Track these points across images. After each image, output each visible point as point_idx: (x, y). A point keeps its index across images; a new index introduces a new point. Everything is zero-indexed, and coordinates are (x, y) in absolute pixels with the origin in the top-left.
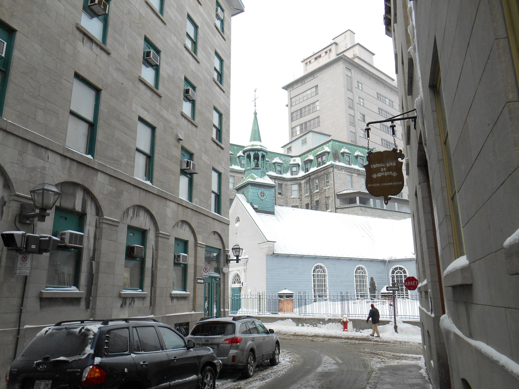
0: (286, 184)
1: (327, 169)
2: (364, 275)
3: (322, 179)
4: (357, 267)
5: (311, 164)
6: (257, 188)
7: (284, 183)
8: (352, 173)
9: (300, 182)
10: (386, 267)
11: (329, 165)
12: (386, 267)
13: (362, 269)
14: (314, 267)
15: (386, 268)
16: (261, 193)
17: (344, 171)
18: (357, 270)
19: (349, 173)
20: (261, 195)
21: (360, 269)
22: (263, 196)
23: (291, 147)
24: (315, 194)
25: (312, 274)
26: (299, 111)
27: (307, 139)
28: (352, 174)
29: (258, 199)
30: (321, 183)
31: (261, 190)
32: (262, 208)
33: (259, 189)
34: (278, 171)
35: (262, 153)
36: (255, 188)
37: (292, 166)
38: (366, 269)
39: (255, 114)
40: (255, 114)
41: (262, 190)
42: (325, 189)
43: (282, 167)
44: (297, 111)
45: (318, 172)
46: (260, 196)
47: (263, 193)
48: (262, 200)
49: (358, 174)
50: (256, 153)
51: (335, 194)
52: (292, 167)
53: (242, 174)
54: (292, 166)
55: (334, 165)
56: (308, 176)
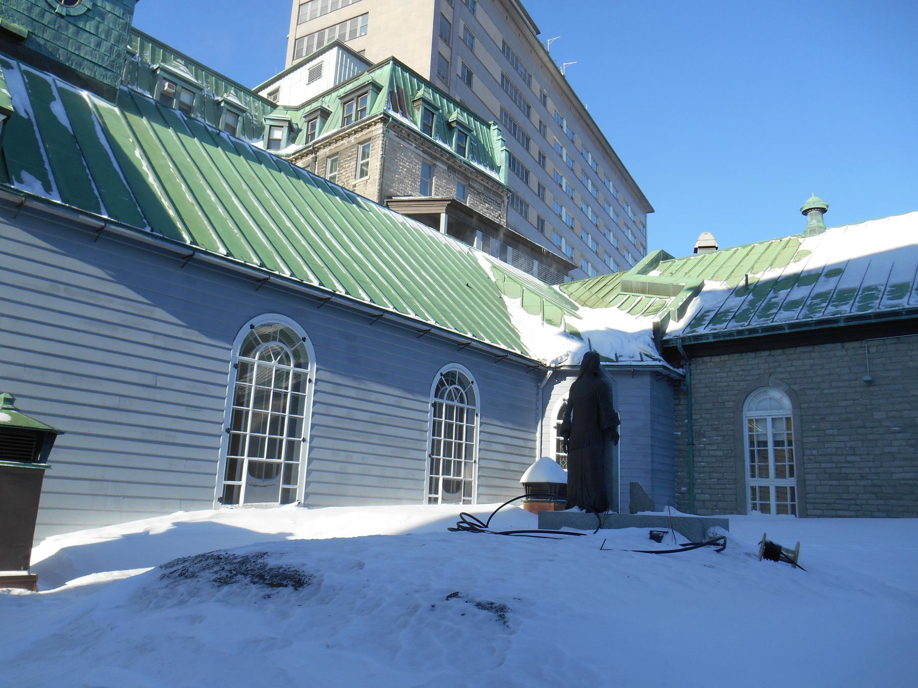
1: (369, 125)
2: (465, 406)
3: (349, 156)
4: (445, 369)
5: (324, 123)
8: (435, 158)
10: (540, 392)
11: (376, 116)
12: (540, 392)
13: (463, 382)
14: (248, 325)
15: (541, 394)
17: (414, 145)
18: (441, 383)
19: (426, 156)
21: (453, 383)
23: (277, 91)
26: (316, 35)
27: (324, 65)
28: (434, 162)
30: (345, 168)
38: (475, 388)
44: (311, 35)
45: (343, 138)
49: (450, 168)
52: (271, 126)
55: (389, 117)
56: (311, 152)
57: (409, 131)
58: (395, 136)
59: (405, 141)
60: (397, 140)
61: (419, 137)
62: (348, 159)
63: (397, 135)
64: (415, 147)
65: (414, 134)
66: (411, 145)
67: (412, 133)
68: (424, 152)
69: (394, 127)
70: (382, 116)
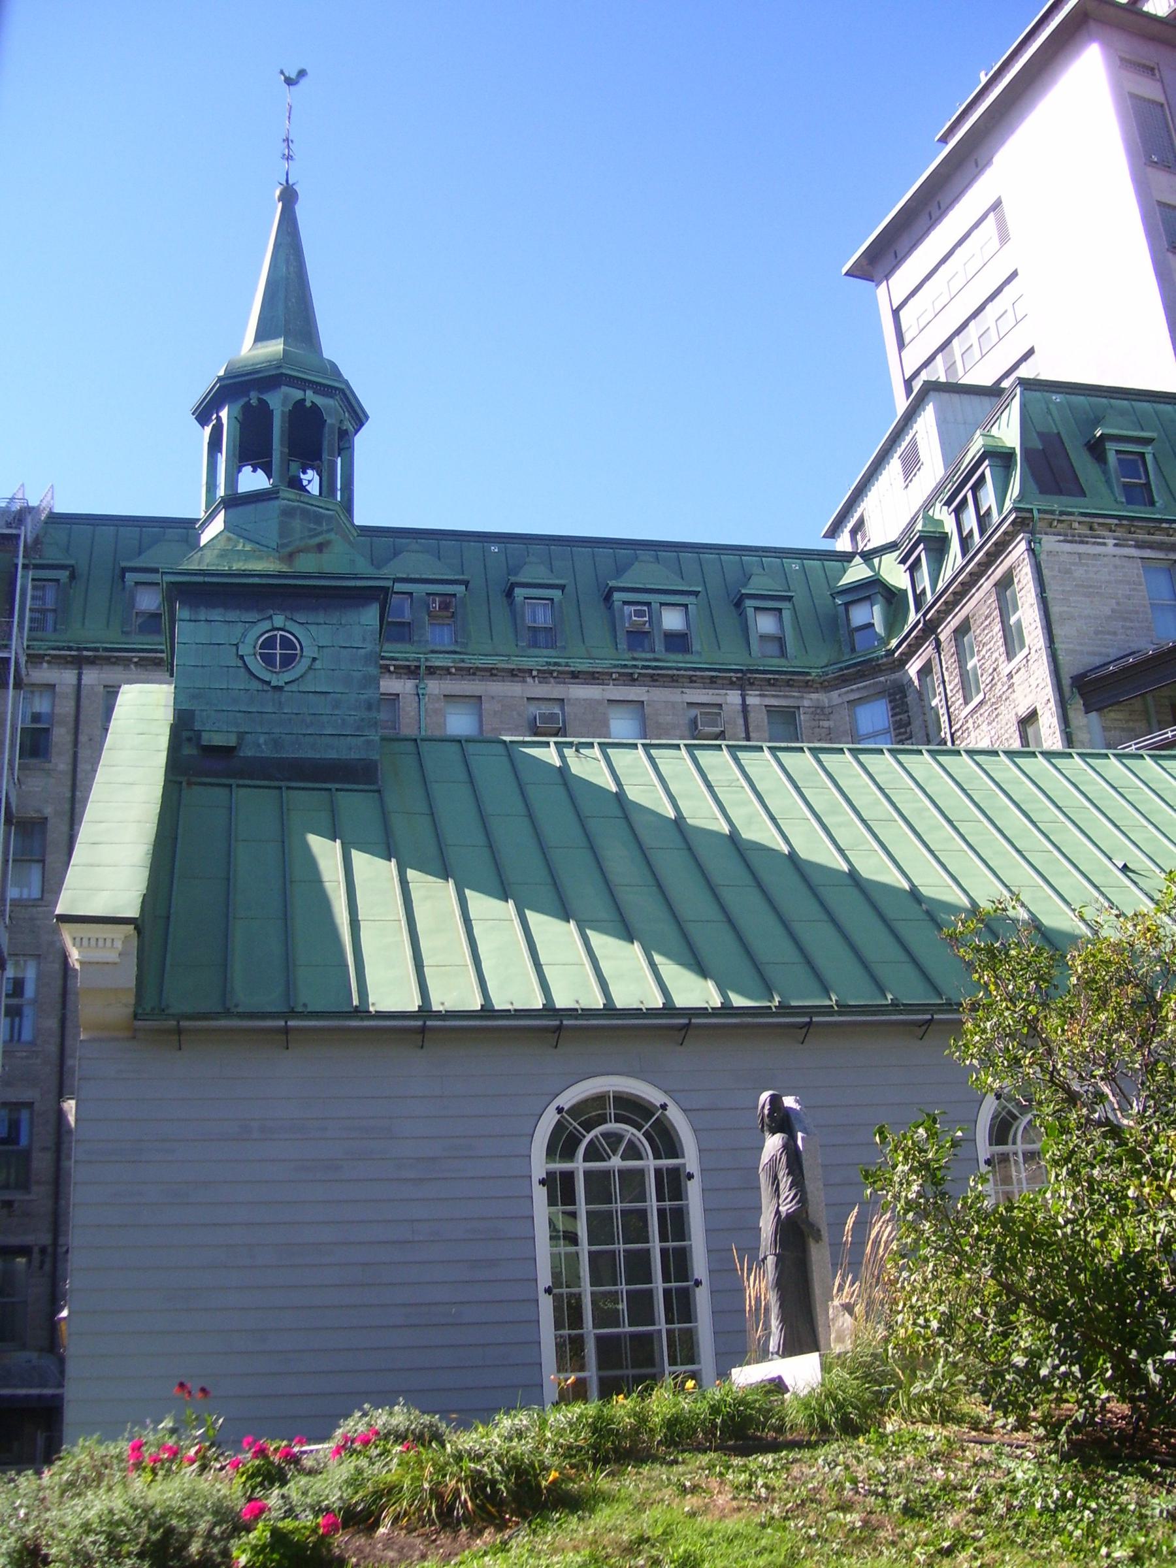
0: (823, 708)
3: (987, 618)
6: (232, 615)
7: (806, 703)
9: (895, 680)
14: (551, 1109)
16: (269, 643)
17: (1111, 542)
19: (1148, 553)
20: (268, 660)
22: (288, 661)
24: (970, 724)
25: (539, 1166)
29: (241, 682)
31: (266, 625)
32: (277, 744)
33: (252, 616)
34: (763, 638)
35: (298, 394)
36: (216, 614)
37: (848, 598)
39: (289, 196)
40: (289, 196)
41: (279, 620)
42: (1006, 672)
43: (786, 614)
46: (256, 665)
47: (286, 643)
48: (278, 689)
50: (254, 402)
51: (1066, 682)
53: (529, 680)
54: (848, 598)
55: (1031, 511)
57: (1087, 519)
58: (1059, 541)
59: (1087, 543)
60: (1067, 547)
61: (1116, 521)
62: (987, 622)
63: (1061, 538)
64: (1116, 545)
65: (1101, 520)
66: (1104, 544)
67: (1096, 520)
68: (1140, 545)
69: (1051, 526)
70: (1014, 516)
